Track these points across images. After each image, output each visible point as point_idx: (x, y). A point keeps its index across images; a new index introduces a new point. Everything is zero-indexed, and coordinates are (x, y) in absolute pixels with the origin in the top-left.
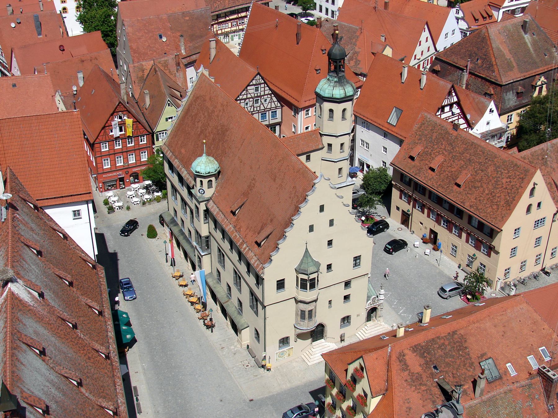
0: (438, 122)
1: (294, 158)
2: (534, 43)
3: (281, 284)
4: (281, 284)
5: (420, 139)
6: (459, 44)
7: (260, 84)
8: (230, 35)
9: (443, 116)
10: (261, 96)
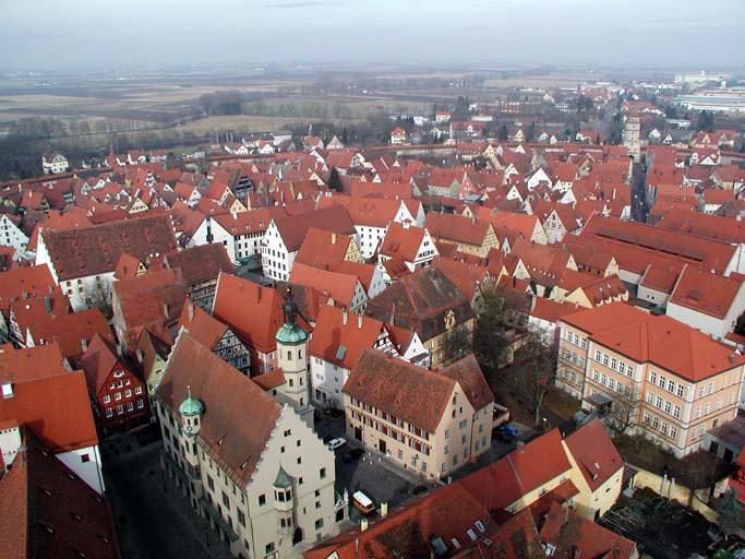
2: (441, 286)
3: (262, 500)
4: (262, 500)
9: (379, 348)
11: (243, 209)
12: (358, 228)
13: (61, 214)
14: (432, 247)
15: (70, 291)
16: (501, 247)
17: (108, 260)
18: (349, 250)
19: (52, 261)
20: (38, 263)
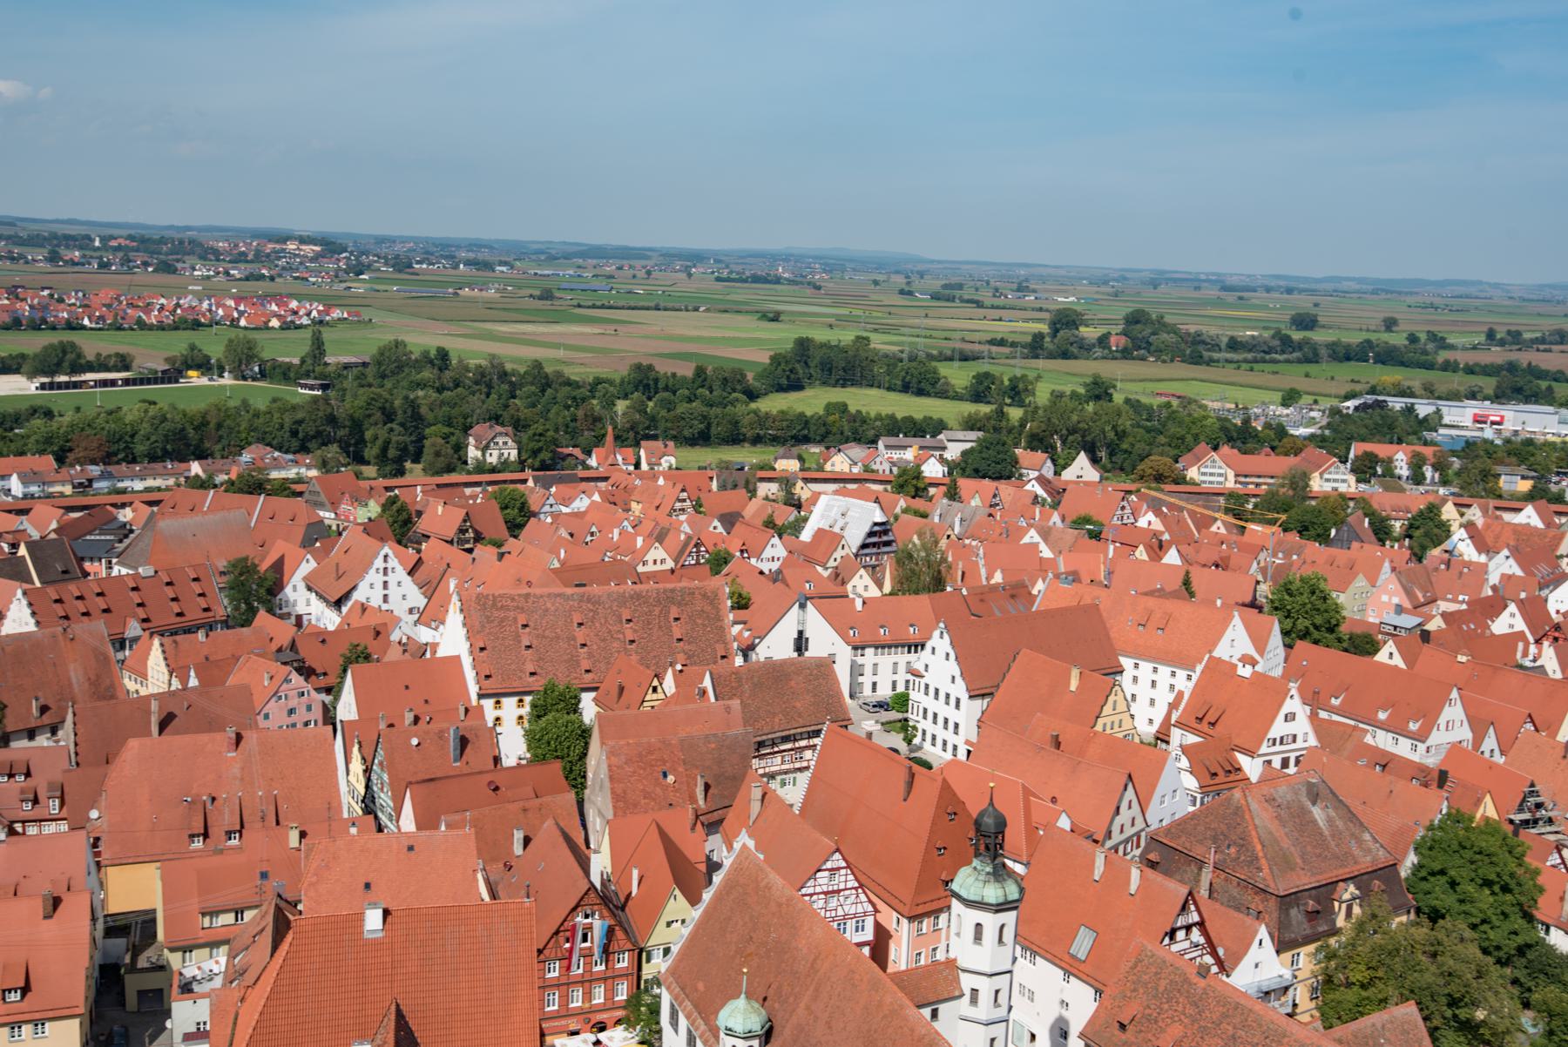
0: (1169, 958)
1: (911, 1010)
2: (1330, 820)
5: (1135, 990)
6: (1193, 816)
7: (839, 869)
8: (779, 778)
9: (1175, 948)
10: (839, 891)
11: (874, 592)
12: (1127, 663)
13: (501, 556)
14: (1302, 726)
15: (498, 719)
16: (1478, 740)
17: (586, 665)
18: (1107, 710)
19: (471, 653)
20: (440, 653)
